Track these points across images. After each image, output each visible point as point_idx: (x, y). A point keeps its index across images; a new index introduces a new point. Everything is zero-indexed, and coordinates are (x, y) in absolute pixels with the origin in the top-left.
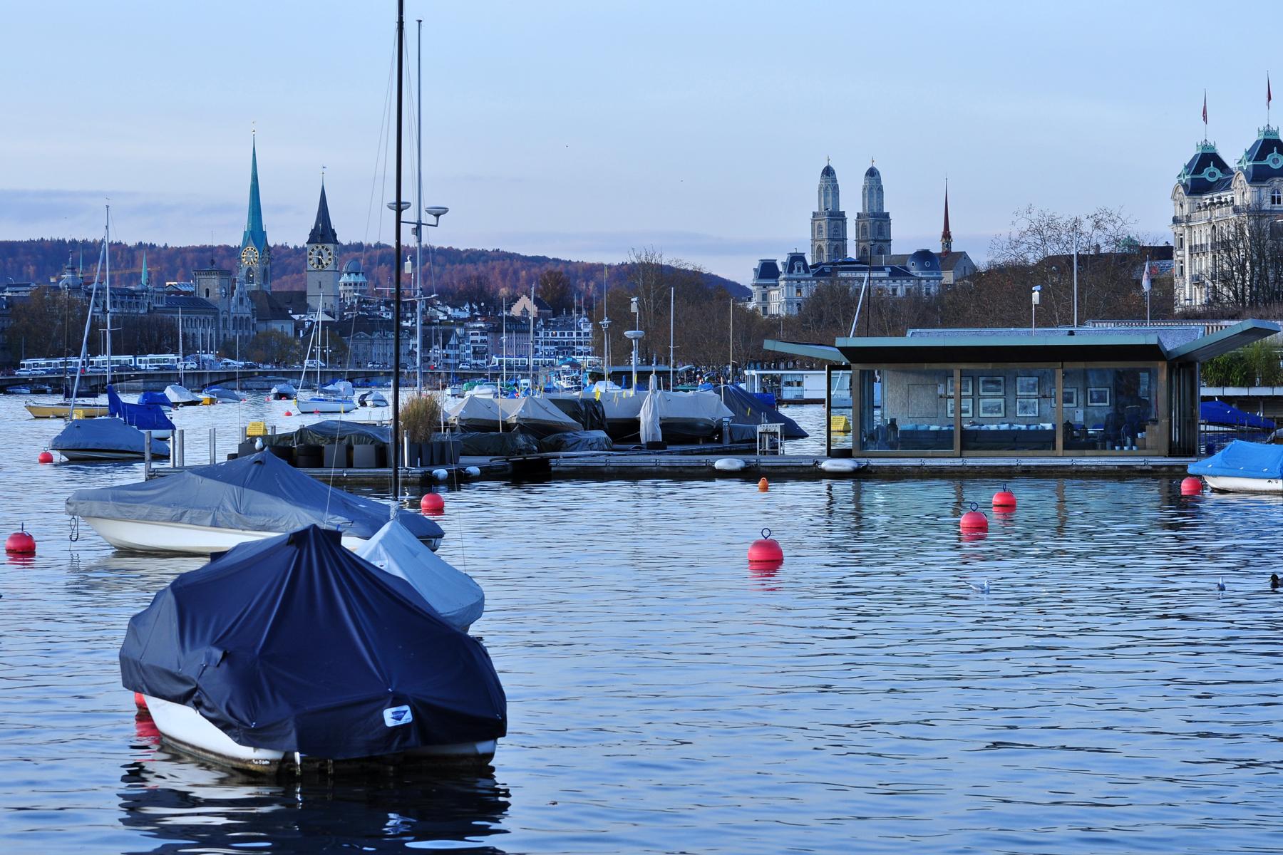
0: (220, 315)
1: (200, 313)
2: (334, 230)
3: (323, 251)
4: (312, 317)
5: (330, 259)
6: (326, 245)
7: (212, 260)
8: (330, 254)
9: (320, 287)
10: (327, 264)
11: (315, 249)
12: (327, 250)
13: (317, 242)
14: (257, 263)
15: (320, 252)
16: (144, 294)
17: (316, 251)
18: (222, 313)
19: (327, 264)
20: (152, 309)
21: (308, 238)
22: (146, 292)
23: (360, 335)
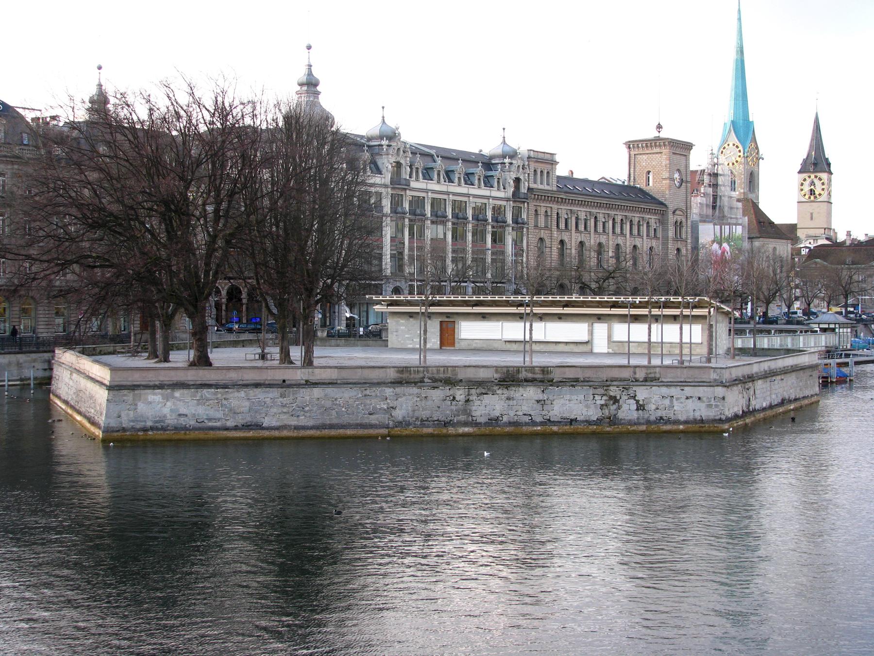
0: (670, 216)
1: (633, 209)
3: (816, 181)
4: (810, 243)
5: (823, 189)
6: (819, 175)
7: (659, 124)
8: (823, 184)
9: (812, 219)
10: (820, 195)
11: (807, 179)
12: (820, 179)
14: (741, 163)
15: (813, 182)
16: (507, 161)
17: (808, 181)
18: (674, 212)
19: (820, 195)
20: (524, 190)
21: (799, 168)
22: (511, 157)
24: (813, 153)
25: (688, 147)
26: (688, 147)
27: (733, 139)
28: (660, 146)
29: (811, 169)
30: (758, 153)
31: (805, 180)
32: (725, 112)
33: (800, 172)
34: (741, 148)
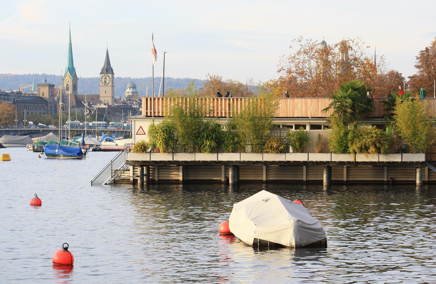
2: (112, 68)
3: (107, 78)
8: (110, 79)
9: (106, 93)
10: (109, 83)
12: (109, 77)
13: (104, 73)
15: (106, 78)
16: (12, 94)
18: (50, 103)
20: (15, 101)
22: (13, 93)
23: (117, 114)
24: (106, 66)
25: (53, 86)
26: (53, 86)
27: (68, 73)
28: (46, 86)
29: (105, 72)
30: (77, 78)
31: (103, 77)
32: (66, 64)
33: (101, 74)
34: (71, 77)
